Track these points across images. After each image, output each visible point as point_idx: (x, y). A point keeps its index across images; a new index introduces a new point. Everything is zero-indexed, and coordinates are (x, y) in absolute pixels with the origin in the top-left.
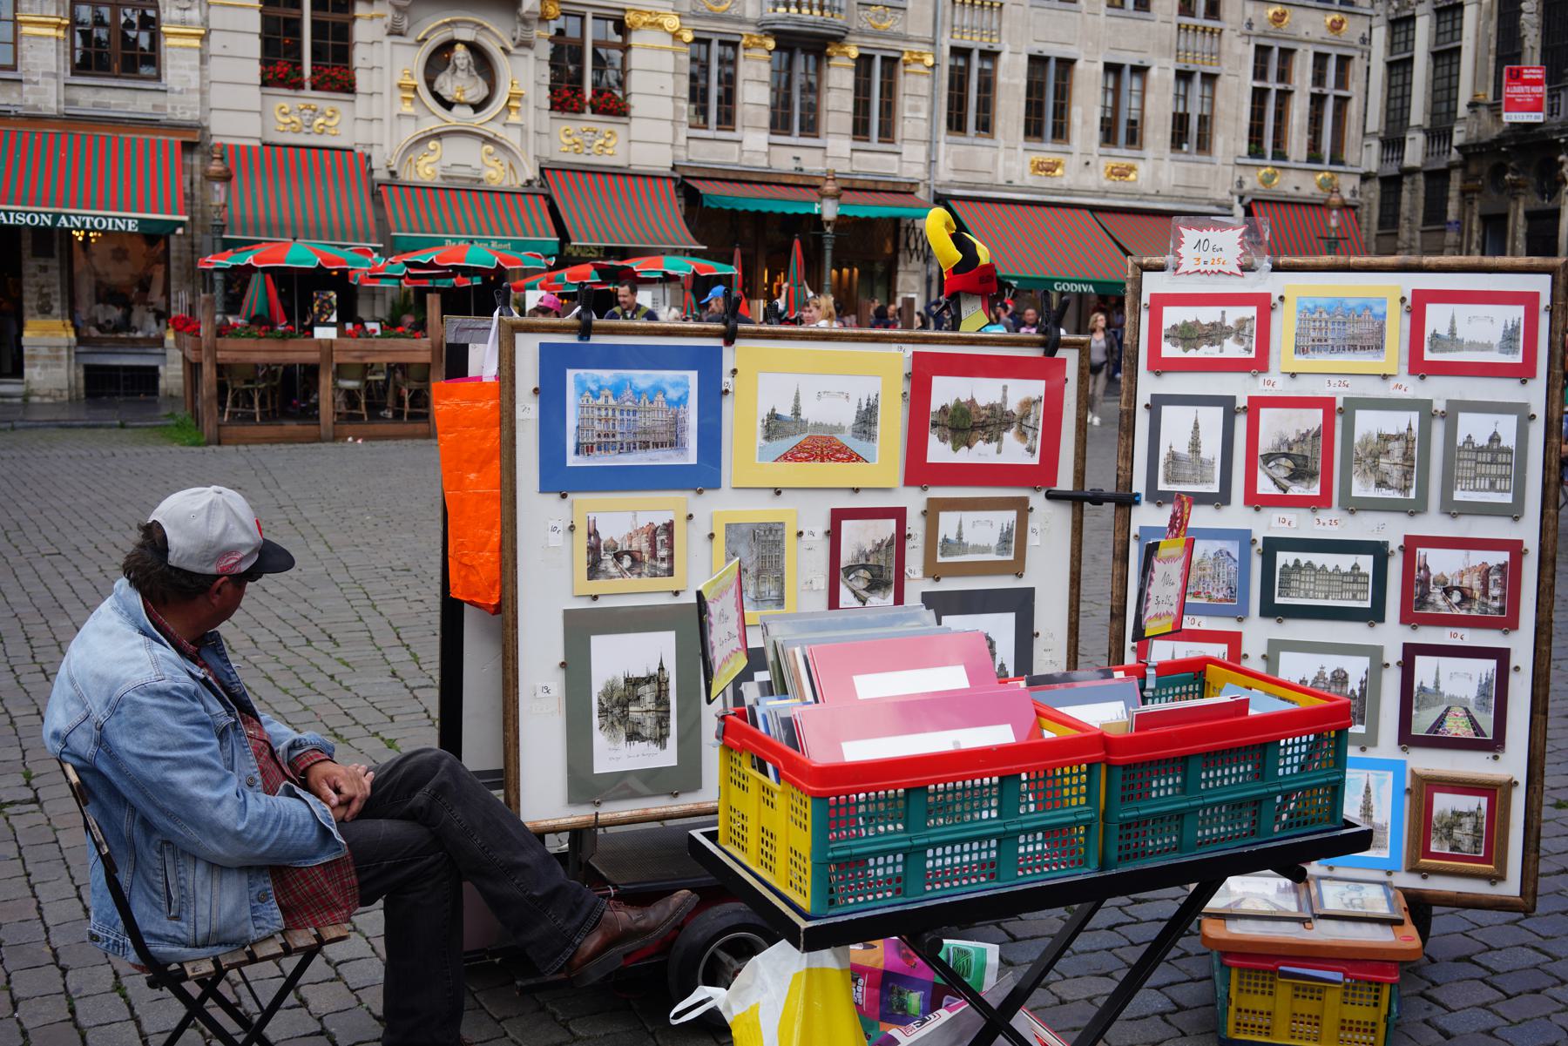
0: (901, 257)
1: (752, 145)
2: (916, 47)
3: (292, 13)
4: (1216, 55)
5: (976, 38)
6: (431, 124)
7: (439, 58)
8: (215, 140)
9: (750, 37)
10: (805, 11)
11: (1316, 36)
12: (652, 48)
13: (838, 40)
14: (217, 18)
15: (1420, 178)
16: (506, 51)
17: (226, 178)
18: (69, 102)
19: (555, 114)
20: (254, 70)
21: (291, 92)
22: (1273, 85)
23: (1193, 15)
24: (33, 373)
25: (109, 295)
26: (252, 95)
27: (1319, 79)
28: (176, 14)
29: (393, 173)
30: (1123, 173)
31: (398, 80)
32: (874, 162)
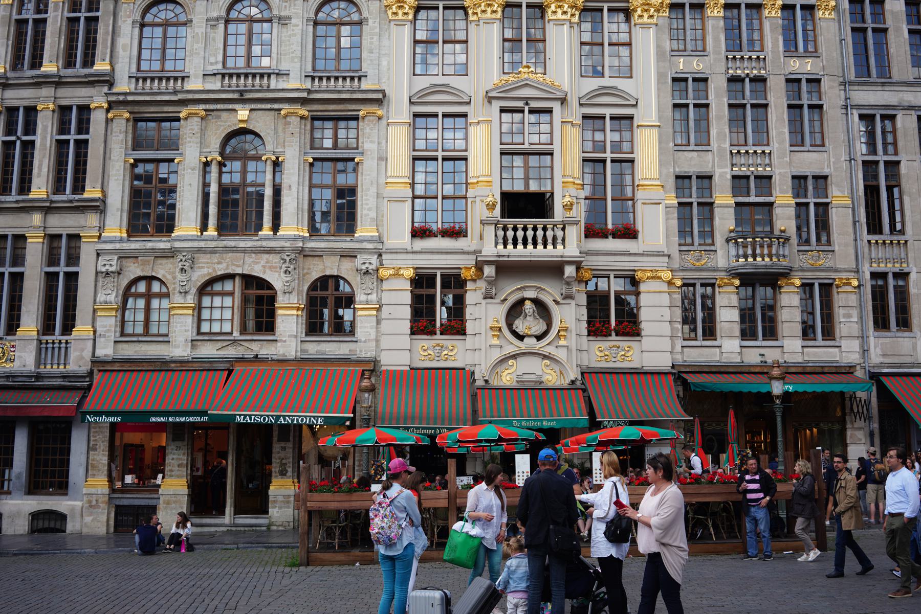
0: (848, 418)
1: (729, 348)
2: (844, 275)
5: (889, 265)
6: (510, 349)
7: (515, 310)
8: (383, 368)
9: (722, 279)
10: (759, 259)
12: (655, 292)
13: (786, 274)
14: (386, 298)
18: (302, 351)
19: (591, 338)
20: (406, 326)
21: (429, 337)
24: (274, 512)
29: (486, 381)
31: (491, 323)
32: (821, 354)
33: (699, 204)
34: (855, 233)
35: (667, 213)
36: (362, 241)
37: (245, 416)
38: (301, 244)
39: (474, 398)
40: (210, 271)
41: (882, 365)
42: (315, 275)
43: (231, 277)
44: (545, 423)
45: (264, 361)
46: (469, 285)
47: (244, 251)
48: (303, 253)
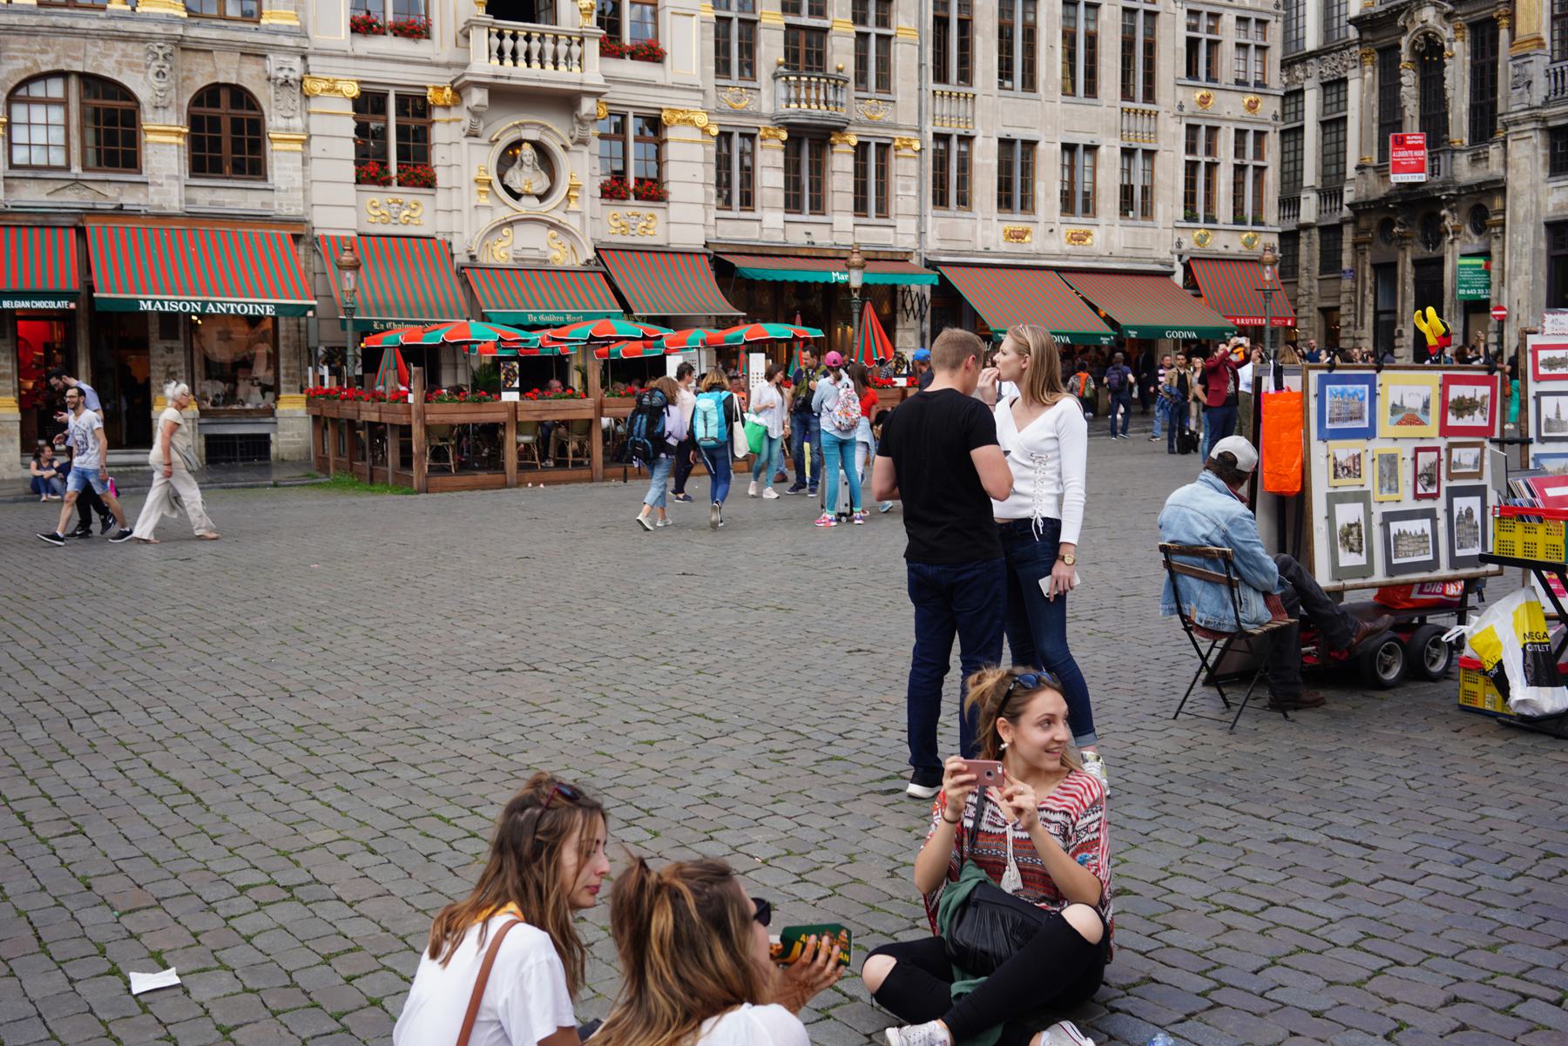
0: (898, 316)
1: (770, 223)
2: (905, 135)
3: (405, 120)
4: (1153, 134)
6: (504, 213)
7: (508, 158)
8: (317, 233)
9: (766, 129)
10: (814, 106)
11: (1236, 115)
12: (685, 141)
13: (840, 130)
14: (317, 125)
15: (1315, 232)
16: (565, 148)
17: (355, 267)
18: (189, 201)
20: (350, 171)
21: (381, 188)
22: (1202, 158)
23: (1133, 100)
25: (213, 370)
26: (348, 192)
27: (1239, 151)
28: (282, 123)
29: (473, 257)
30: (1079, 238)
31: (475, 175)
32: (874, 235)
33: (740, 20)
34: (920, 80)
35: (702, 30)
36: (276, 33)
37: (154, 301)
38: (180, 31)
39: (465, 283)
40: (29, 64)
41: (939, 252)
42: (201, 82)
43: (63, 75)
44: (542, 318)
45: (134, 215)
46: (438, 114)
47: (86, 34)
48: (183, 46)
